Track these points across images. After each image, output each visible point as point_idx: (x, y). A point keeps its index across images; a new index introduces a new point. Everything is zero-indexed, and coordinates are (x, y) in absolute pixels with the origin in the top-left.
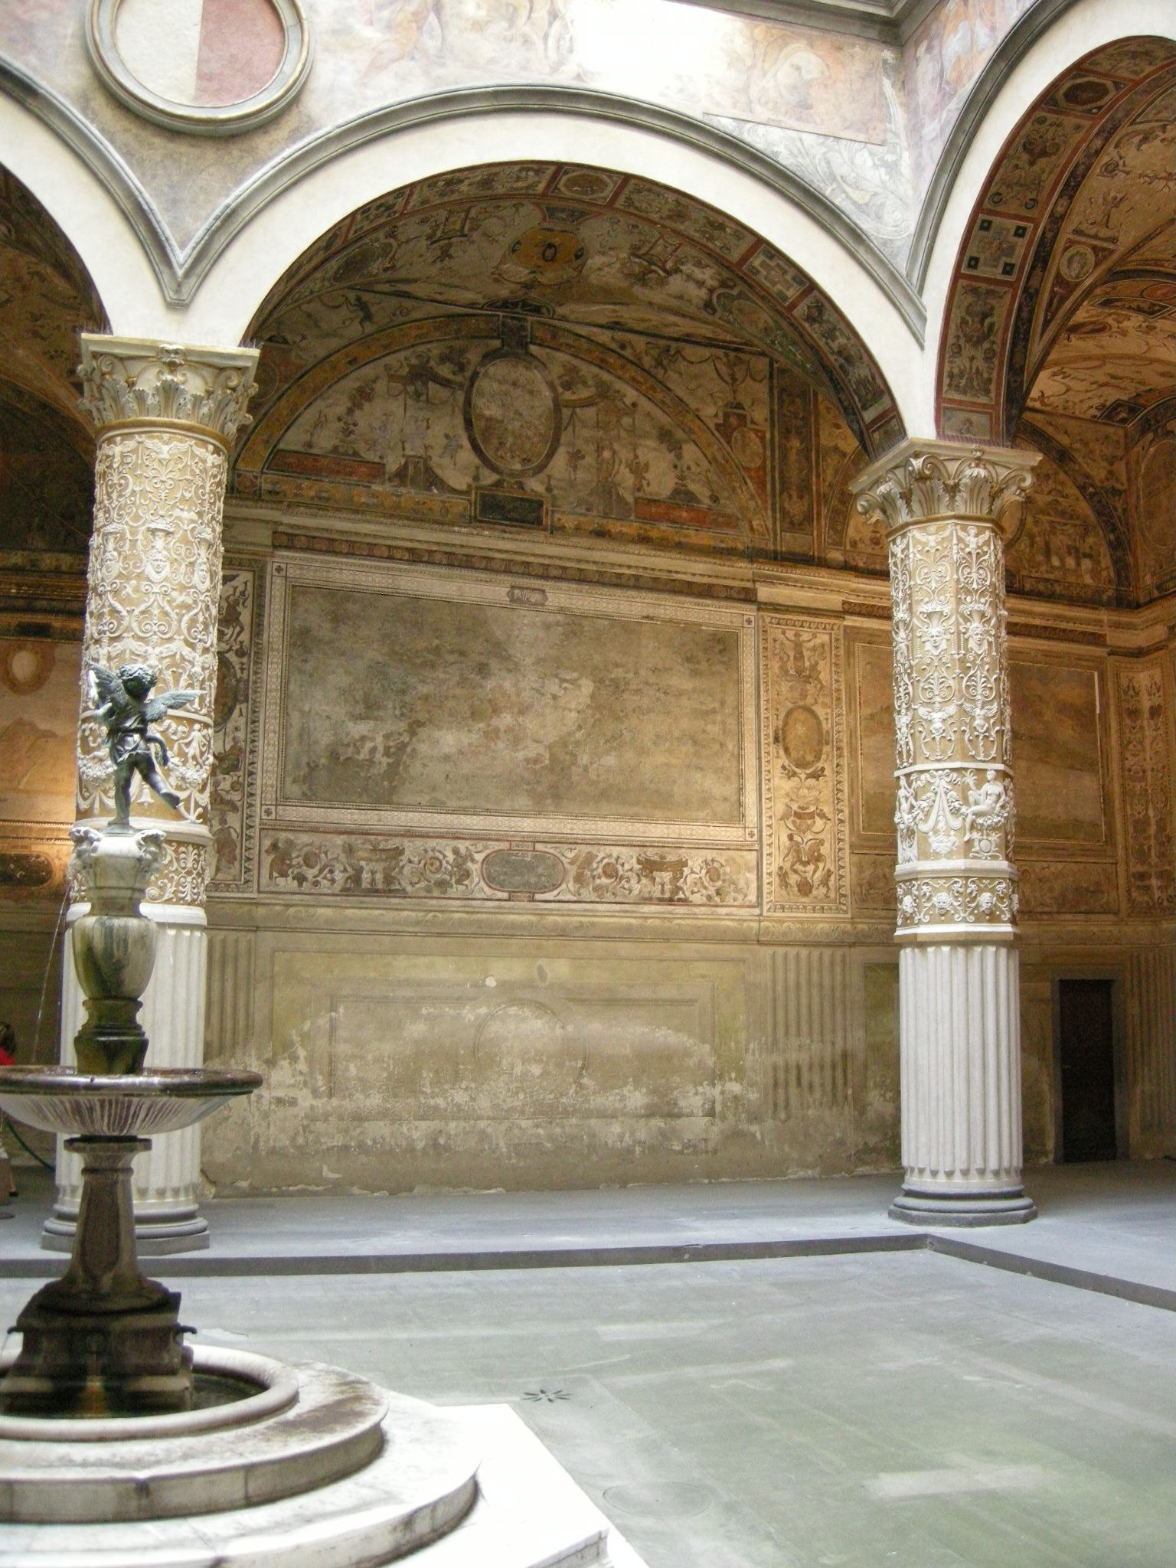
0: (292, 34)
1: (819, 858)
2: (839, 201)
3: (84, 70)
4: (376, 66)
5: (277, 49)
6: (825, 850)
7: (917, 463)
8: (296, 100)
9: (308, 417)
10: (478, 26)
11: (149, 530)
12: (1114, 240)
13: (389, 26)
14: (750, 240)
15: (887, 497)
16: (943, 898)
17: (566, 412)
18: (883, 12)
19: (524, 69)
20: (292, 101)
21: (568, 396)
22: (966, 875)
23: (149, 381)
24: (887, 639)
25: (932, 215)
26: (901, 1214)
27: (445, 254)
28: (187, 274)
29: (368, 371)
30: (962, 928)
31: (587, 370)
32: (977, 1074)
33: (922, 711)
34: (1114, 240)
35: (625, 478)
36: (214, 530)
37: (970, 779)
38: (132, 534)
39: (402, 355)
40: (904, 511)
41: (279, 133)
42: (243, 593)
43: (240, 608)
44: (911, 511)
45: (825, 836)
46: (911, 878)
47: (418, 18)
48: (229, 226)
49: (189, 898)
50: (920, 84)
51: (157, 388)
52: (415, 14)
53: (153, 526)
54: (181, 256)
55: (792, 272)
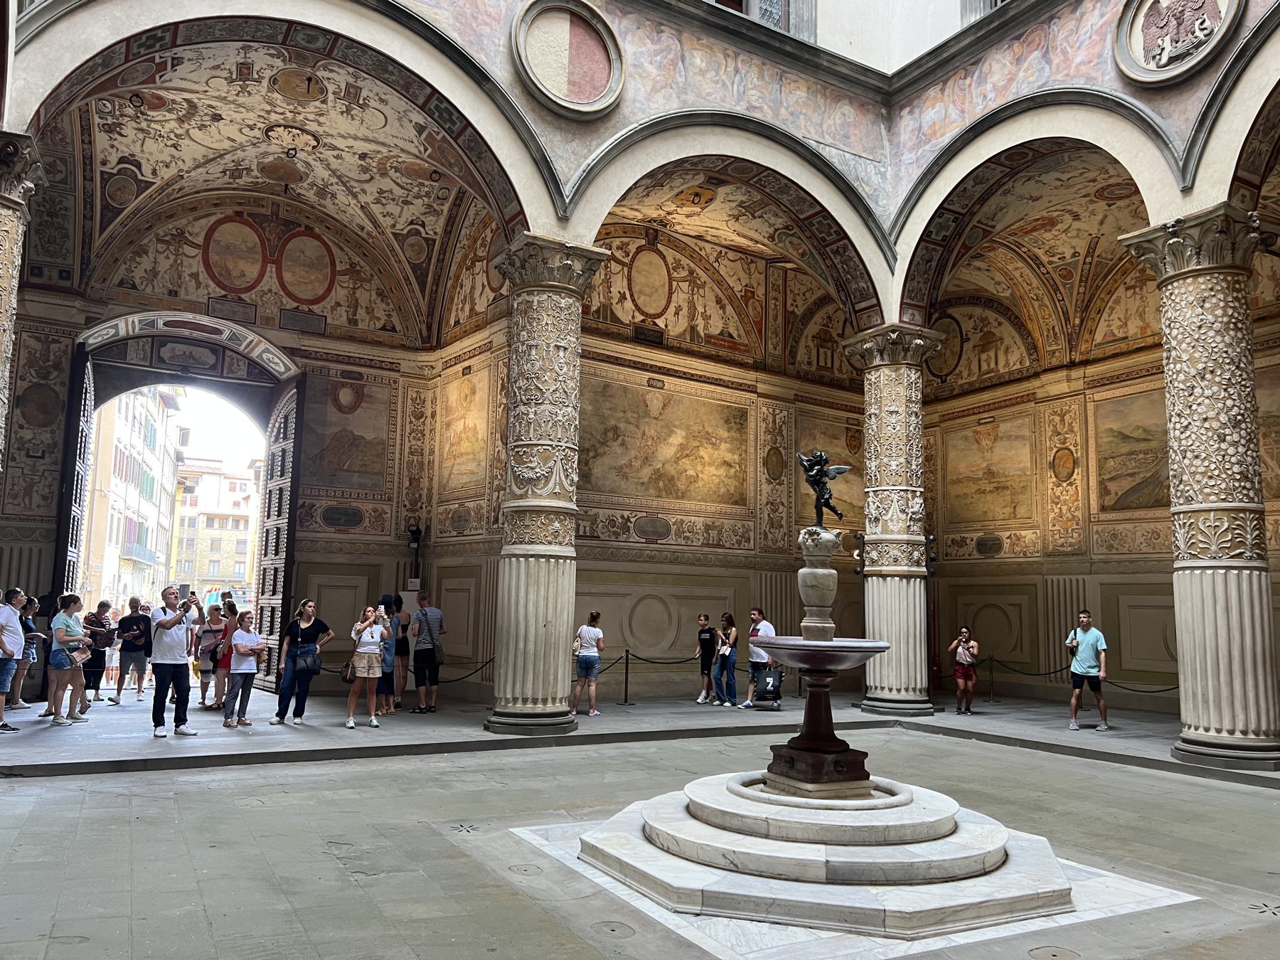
0: (616, 64)
1: (781, 526)
2: (860, 190)
4: (655, 90)
5: (605, 75)
6: (784, 522)
7: (894, 336)
8: (618, 105)
10: (702, 73)
12: (993, 227)
13: (660, 67)
14: (819, 208)
15: (869, 351)
16: (895, 552)
17: (675, 284)
18: (886, 87)
19: (723, 101)
20: (614, 108)
21: (675, 274)
22: (908, 543)
23: (556, 262)
24: (860, 423)
25: (909, 205)
26: (873, 710)
30: (906, 568)
31: (685, 261)
32: (911, 641)
33: (885, 460)
34: (993, 227)
35: (700, 322)
37: (910, 496)
40: (878, 358)
44: (882, 359)
45: (784, 515)
46: (876, 543)
48: (589, 177)
50: (902, 131)
54: (567, 190)
55: (835, 228)
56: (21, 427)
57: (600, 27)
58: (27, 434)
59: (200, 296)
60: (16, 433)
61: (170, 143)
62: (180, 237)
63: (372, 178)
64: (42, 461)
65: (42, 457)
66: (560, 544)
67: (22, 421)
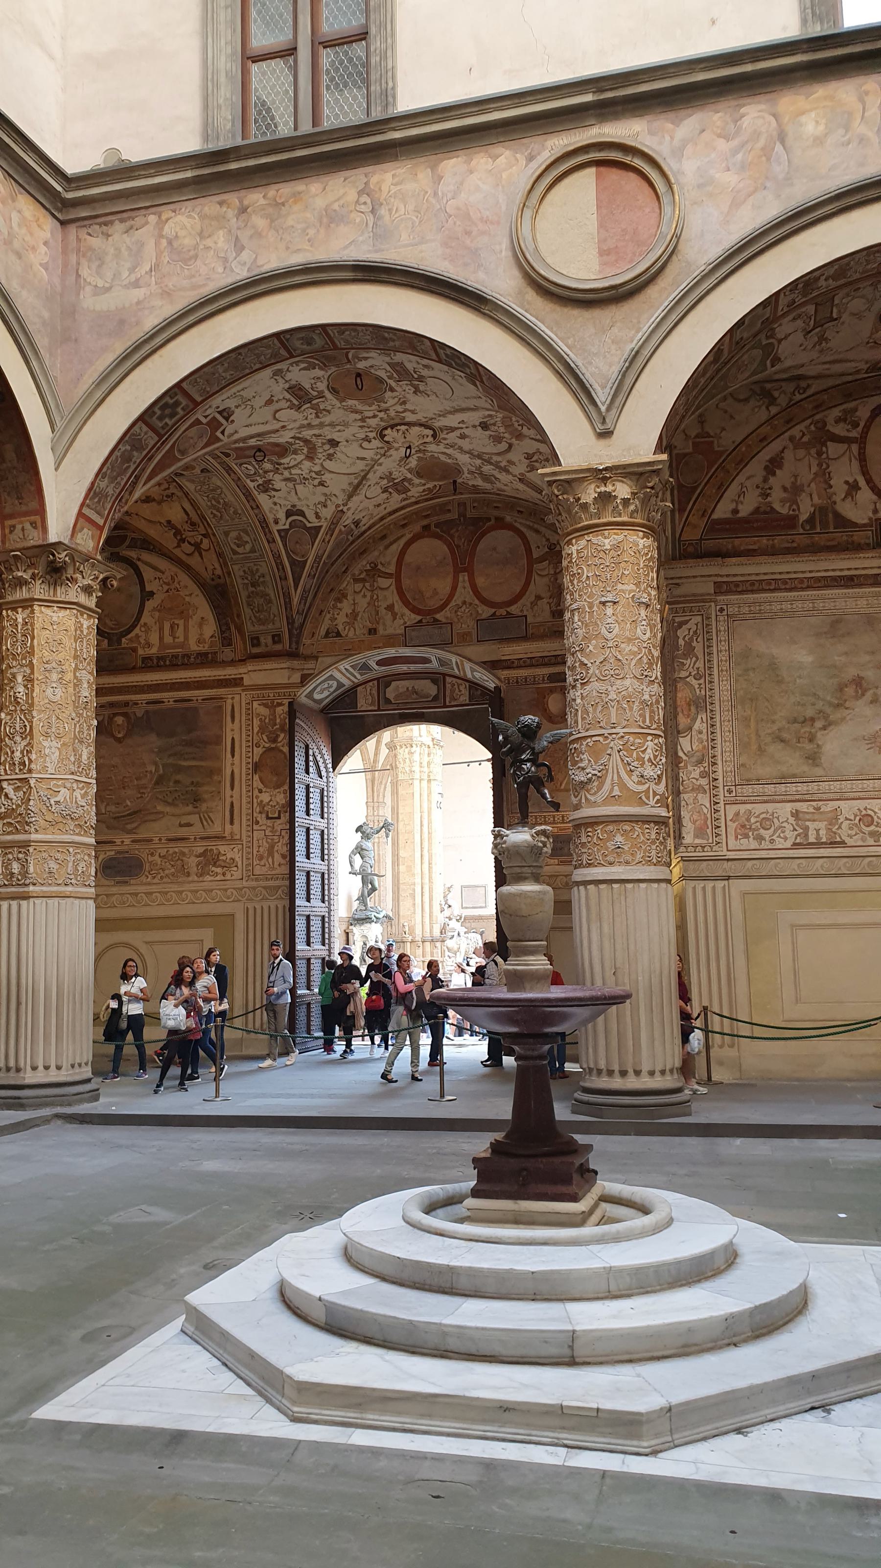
0: (665, 199)
3: (516, 273)
4: (736, 204)
8: (672, 253)
9: (733, 491)
10: (819, 141)
11: (600, 602)
27: (822, 339)
28: (608, 409)
29: (775, 447)
36: (649, 594)
38: (590, 608)
39: (802, 427)
41: (663, 282)
42: (695, 632)
43: (694, 644)
47: (767, 152)
48: (635, 365)
49: (654, 861)
51: (595, 498)
52: (763, 149)
53: (603, 599)
54: (602, 396)
56: (260, 791)
57: (638, 162)
58: (265, 797)
59: (395, 627)
60: (257, 797)
61: (316, 482)
62: (374, 571)
63: (510, 446)
64: (279, 821)
65: (279, 818)
66: (627, 863)
67: (261, 786)
